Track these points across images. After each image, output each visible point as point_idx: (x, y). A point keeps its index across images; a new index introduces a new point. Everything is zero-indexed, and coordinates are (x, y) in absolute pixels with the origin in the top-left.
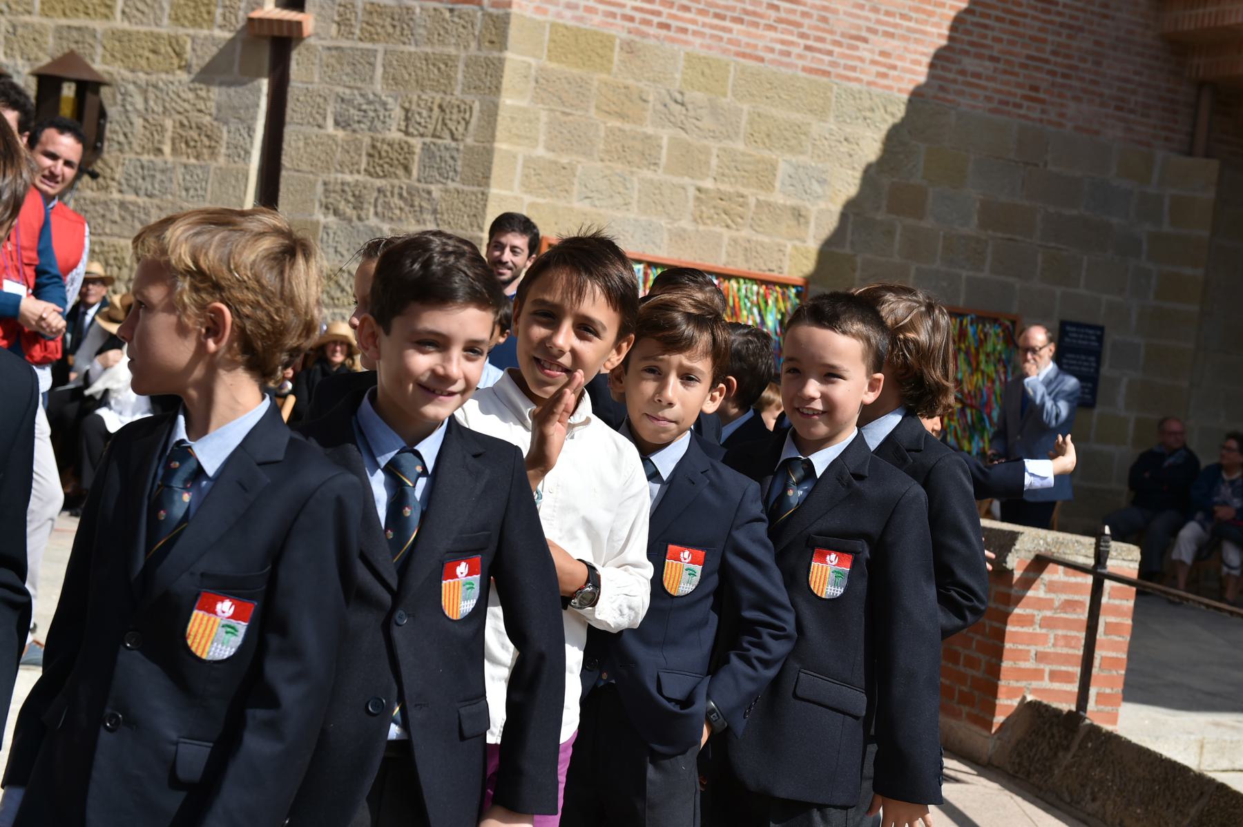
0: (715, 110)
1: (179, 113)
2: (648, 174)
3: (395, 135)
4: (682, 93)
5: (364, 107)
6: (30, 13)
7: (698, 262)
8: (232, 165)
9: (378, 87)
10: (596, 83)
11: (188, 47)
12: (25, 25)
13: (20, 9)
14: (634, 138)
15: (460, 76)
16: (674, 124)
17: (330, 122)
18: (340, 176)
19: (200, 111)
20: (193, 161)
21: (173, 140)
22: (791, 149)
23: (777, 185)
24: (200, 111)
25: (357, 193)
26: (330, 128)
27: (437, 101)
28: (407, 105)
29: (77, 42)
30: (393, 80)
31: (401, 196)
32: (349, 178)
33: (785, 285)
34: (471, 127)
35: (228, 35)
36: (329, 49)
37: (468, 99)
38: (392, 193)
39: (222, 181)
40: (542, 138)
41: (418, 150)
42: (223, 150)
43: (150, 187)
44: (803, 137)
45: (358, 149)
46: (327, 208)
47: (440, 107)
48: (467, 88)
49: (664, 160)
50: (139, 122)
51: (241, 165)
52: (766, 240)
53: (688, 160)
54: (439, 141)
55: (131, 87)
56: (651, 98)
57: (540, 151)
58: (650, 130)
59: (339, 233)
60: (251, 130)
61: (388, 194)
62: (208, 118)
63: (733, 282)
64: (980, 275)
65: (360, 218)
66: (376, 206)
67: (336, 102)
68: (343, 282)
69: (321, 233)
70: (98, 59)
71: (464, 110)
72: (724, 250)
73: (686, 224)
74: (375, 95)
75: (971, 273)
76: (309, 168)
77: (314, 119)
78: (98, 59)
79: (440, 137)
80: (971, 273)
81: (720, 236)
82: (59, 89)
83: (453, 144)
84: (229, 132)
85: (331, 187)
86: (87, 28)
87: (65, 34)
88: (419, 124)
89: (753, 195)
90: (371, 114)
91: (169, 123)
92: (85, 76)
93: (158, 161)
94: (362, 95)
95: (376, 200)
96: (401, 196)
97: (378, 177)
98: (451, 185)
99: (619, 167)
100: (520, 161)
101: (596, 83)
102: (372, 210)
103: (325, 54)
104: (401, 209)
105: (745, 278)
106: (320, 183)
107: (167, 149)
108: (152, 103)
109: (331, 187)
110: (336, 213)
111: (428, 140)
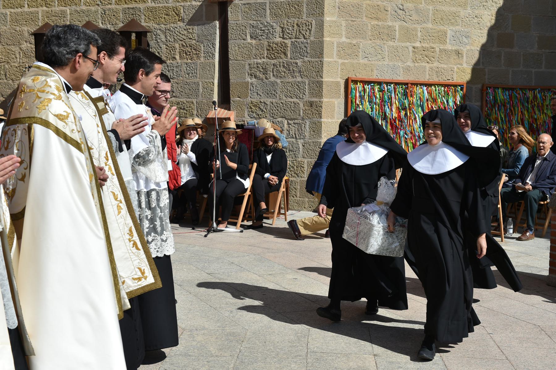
0: (417, 10)
1: (181, 41)
2: (391, 43)
3: (278, 40)
4: (402, 5)
5: (263, 29)
6: (110, 4)
7: (416, 80)
8: (207, 61)
9: (268, 19)
10: (365, 6)
11: (182, 11)
12: (109, 9)
13: (106, 3)
14: (384, 28)
15: (305, 10)
16: (401, 20)
17: (248, 37)
18: (255, 60)
19: (190, 39)
20: (189, 61)
21: (180, 53)
22: (452, 24)
23: (448, 41)
24: (190, 39)
26: (249, 40)
27: (296, 22)
28: (282, 26)
29: (133, 14)
30: (275, 15)
31: (284, 66)
32: (260, 61)
33: (455, 86)
34: (312, 32)
35: (199, 4)
36: (244, 4)
37: (310, 20)
39: (203, 68)
40: (344, 33)
41: (289, 45)
42: (202, 55)
43: (172, 75)
44: (457, 18)
45: (262, 48)
46: (251, 75)
47: (297, 24)
48: (308, 15)
49: (397, 36)
50: (164, 47)
51: (211, 60)
52: (445, 66)
53: (408, 35)
54: (299, 40)
55: (159, 31)
56: (389, 9)
57: (344, 39)
58: (390, 24)
60: (214, 45)
62: (194, 41)
63: (433, 87)
64: (541, 70)
65: (266, 78)
66: (273, 72)
67: (250, 28)
68: (262, 108)
70: (143, 21)
71: (309, 25)
72: (427, 73)
73: (409, 63)
74: (267, 22)
75: (536, 70)
76: (242, 59)
77: (241, 36)
78: (143, 21)
79: (299, 38)
80: (536, 70)
81: (425, 66)
82: (131, 35)
83: (305, 41)
84: (204, 47)
85: (252, 66)
86: (136, 7)
87: (127, 12)
88: (289, 33)
89: (438, 47)
90: (267, 31)
91: (177, 46)
92: (141, 30)
93: (174, 62)
94: (261, 23)
95: (273, 69)
96: (284, 66)
97: (273, 59)
98: (306, 59)
99: (378, 42)
100: (335, 45)
101: (365, 6)
102: (272, 74)
103: (243, 7)
104: (284, 72)
105: (437, 85)
107: (177, 57)
108: (168, 38)
109: (252, 66)
110: (255, 77)
111: (293, 40)
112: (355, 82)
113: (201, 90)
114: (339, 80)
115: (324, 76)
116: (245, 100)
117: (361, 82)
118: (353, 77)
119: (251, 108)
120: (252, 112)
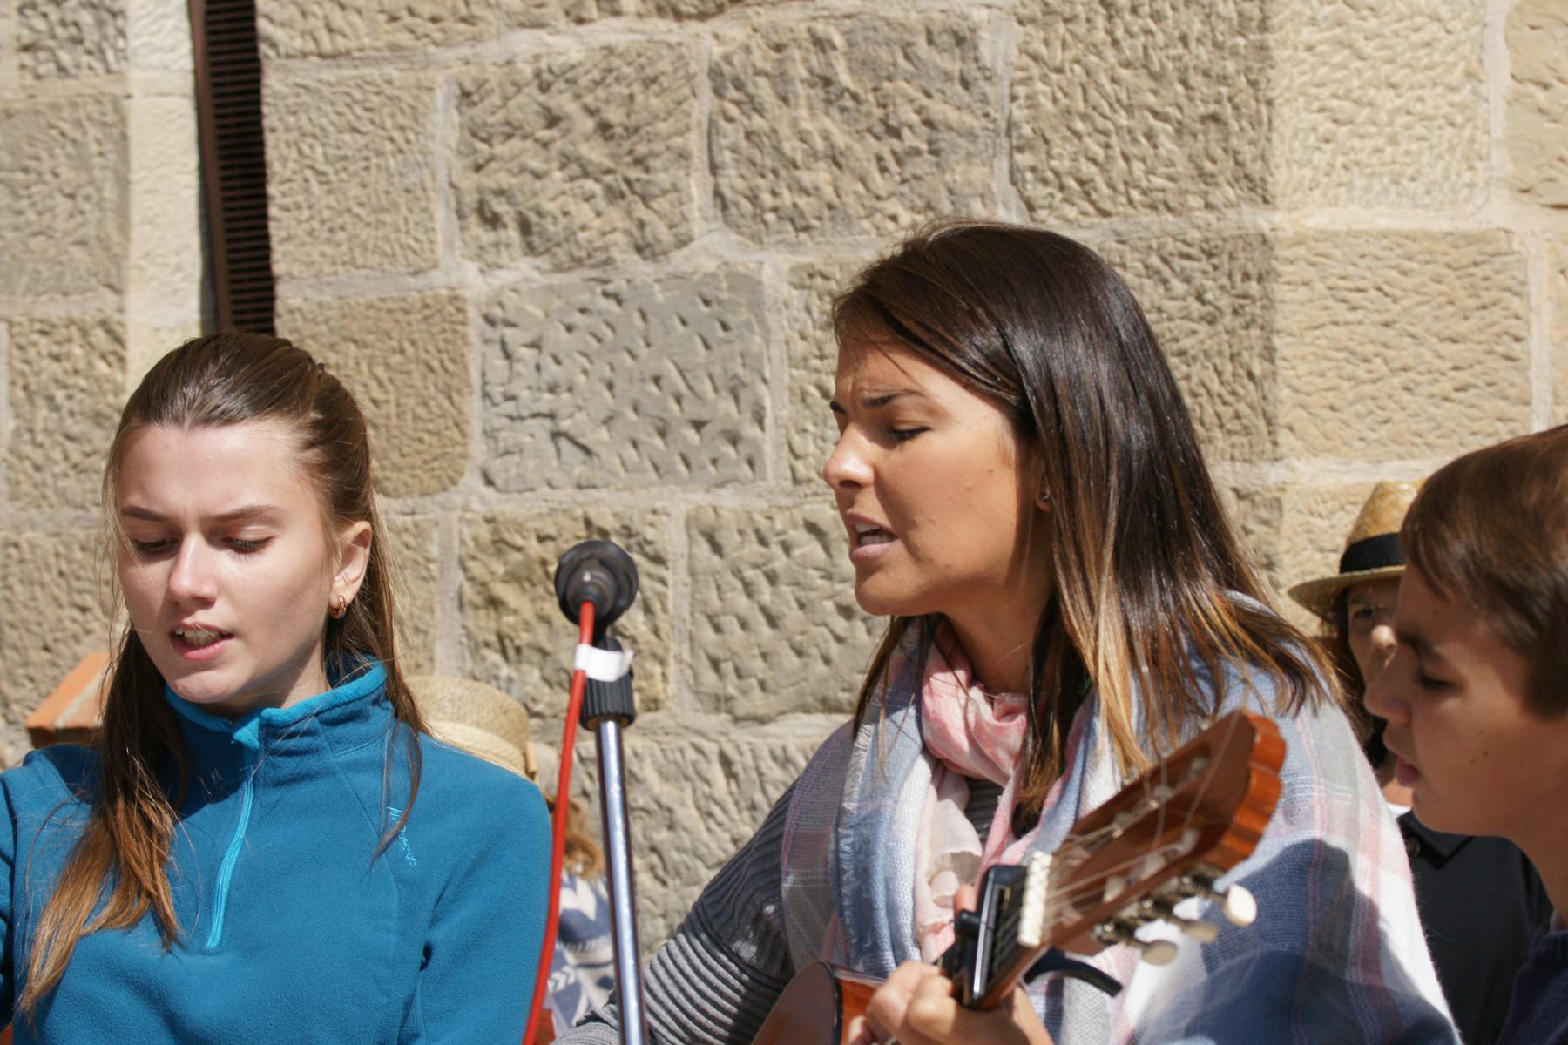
8: (58, 89)
18: (524, 43)
25: (615, 115)
32: (568, 46)
38: (780, 78)
59: (558, 337)
61: (764, 90)
69: (479, 357)
102: (697, 187)
104: (835, 160)
106: (443, 96)
114: (1498, 212)
115: (1280, 180)
116: (431, 509)
119: (494, 603)
120: (503, 644)
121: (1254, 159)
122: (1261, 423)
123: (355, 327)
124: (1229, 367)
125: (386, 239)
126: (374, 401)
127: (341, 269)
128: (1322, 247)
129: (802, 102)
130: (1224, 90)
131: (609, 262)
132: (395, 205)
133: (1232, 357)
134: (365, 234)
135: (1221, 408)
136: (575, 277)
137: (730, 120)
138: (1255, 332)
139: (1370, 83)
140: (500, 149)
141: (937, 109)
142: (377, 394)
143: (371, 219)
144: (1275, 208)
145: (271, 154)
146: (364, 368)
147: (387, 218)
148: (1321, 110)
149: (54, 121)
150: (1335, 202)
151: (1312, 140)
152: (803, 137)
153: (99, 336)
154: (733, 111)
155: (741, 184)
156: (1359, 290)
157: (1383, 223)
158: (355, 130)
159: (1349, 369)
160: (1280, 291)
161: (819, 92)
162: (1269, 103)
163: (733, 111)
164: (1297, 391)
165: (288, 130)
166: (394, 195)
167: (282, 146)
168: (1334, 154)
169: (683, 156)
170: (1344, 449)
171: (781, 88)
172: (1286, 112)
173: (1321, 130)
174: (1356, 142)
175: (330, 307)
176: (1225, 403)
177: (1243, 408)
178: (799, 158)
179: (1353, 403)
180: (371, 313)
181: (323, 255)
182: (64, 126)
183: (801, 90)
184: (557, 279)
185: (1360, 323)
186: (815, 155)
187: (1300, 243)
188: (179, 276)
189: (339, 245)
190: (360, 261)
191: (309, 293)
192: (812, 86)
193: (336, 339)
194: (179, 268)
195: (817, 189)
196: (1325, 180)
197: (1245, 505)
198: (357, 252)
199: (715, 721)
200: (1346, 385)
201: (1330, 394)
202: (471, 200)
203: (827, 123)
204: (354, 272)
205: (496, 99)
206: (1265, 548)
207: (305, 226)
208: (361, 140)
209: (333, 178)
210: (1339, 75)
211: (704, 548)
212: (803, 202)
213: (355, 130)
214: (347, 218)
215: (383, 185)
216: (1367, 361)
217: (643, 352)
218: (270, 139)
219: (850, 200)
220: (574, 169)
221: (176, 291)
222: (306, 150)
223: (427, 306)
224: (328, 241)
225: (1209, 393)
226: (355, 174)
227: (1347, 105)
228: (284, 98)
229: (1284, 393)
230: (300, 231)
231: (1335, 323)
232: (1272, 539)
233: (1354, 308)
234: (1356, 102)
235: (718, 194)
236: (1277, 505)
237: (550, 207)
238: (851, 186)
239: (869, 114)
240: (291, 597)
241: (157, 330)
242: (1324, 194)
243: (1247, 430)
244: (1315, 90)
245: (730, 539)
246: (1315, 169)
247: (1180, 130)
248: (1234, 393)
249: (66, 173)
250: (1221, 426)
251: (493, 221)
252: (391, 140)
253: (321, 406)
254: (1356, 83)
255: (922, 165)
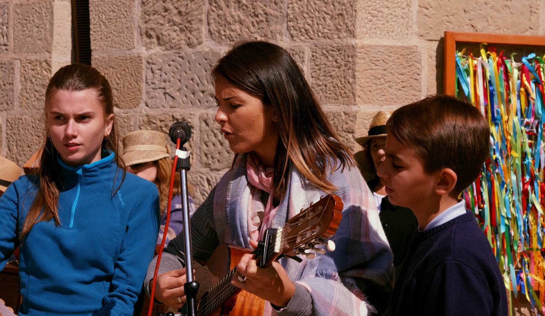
25: (183, 9)
69: (145, 73)
102: (204, 29)
104: (241, 22)
112: (471, 48)
113: (18, 86)
114: (414, 41)
115: (358, 31)
116: (132, 112)
117: (491, 47)
118: (464, 29)
121: (351, 26)
122: (351, 95)
123: (112, 64)
124: (343, 80)
125: (121, 40)
126: (117, 83)
127: (109, 48)
128: (368, 49)
129: (233, 7)
130: (344, 7)
131: (180, 48)
132: (124, 31)
133: (344, 77)
134: (115, 39)
135: (341, 91)
136: (171, 52)
137: (213, 11)
138: (350, 71)
139: (382, 6)
140: (152, 17)
141: (268, 10)
142: (118, 81)
143: (117, 35)
144: (356, 39)
145: (91, 17)
146: (115, 74)
147: (122, 35)
148: (369, 13)
149: (33, 7)
150: (372, 37)
151: (366, 21)
152: (232, 17)
153: (44, 64)
154: (214, 9)
155: (215, 28)
156: (378, 61)
157: (385, 43)
158: (113, 11)
159: (375, 81)
160: (357, 60)
161: (237, 5)
162: (355, 11)
163: (214, 9)
164: (361, 87)
165: (96, 11)
166: (123, 29)
167: (94, 15)
168: (372, 25)
169: (201, 20)
170: (373, 102)
171: (227, 3)
172: (360, 13)
173: (369, 18)
174: (378, 22)
175: (106, 58)
176: (342, 89)
177: (347, 91)
178: (231, 22)
179: (375, 90)
180: (117, 60)
181: (104, 44)
182: (36, 8)
183: (232, 4)
184: (166, 52)
185: (378, 69)
186: (236, 21)
187: (362, 48)
188: (66, 49)
189: (109, 42)
190: (114, 46)
191: (100, 54)
192: (235, 3)
193: (107, 67)
194: (66, 47)
195: (236, 30)
196: (369, 31)
197: (347, 116)
198: (113, 44)
199: (205, 170)
200: (374, 85)
201: (370, 88)
202: (144, 31)
203: (239, 13)
204: (112, 49)
205: (151, 4)
206: (352, 128)
207: (100, 36)
208: (115, 14)
209: (107, 24)
210: (374, 4)
211: (204, 124)
212: (232, 33)
213: (113, 11)
214: (111, 35)
215: (121, 26)
216: (379, 79)
217: (189, 72)
218: (91, 13)
219: (244, 33)
220: (172, 23)
221: (65, 53)
222: (100, 16)
223: (132, 59)
224: (106, 41)
225: (338, 87)
226: (113, 23)
227: (376, 12)
228: (95, 2)
229: (358, 87)
230: (98, 38)
231: (371, 69)
232: (354, 125)
233: (376, 65)
234: (378, 11)
235: (210, 31)
236: (355, 116)
237: (165, 33)
238: (245, 30)
239: (250, 11)
240: (95, 135)
241: (60, 63)
242: (369, 35)
243: (348, 97)
244: (367, 8)
245: (211, 122)
246: (367, 28)
247: (332, 17)
248: (344, 87)
249: (36, 21)
250: (341, 95)
251: (150, 36)
252: (123, 14)
253: (103, 85)
254: (378, 6)
255: (264, 25)
